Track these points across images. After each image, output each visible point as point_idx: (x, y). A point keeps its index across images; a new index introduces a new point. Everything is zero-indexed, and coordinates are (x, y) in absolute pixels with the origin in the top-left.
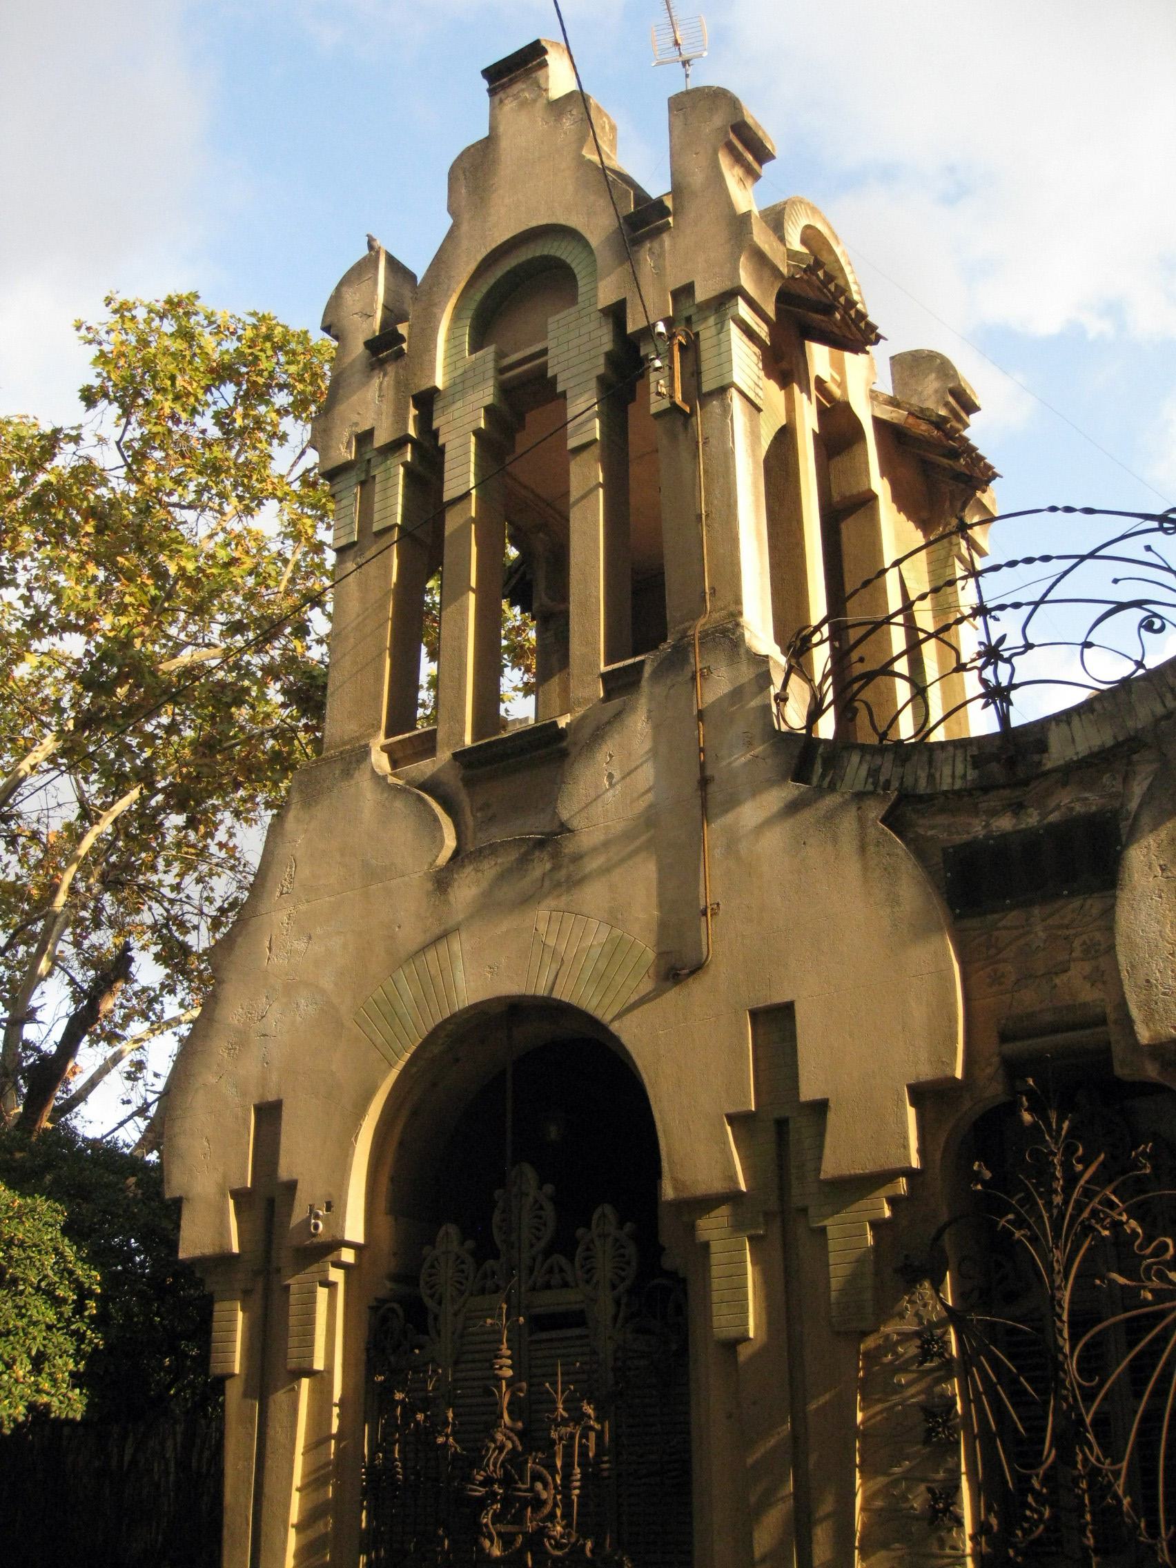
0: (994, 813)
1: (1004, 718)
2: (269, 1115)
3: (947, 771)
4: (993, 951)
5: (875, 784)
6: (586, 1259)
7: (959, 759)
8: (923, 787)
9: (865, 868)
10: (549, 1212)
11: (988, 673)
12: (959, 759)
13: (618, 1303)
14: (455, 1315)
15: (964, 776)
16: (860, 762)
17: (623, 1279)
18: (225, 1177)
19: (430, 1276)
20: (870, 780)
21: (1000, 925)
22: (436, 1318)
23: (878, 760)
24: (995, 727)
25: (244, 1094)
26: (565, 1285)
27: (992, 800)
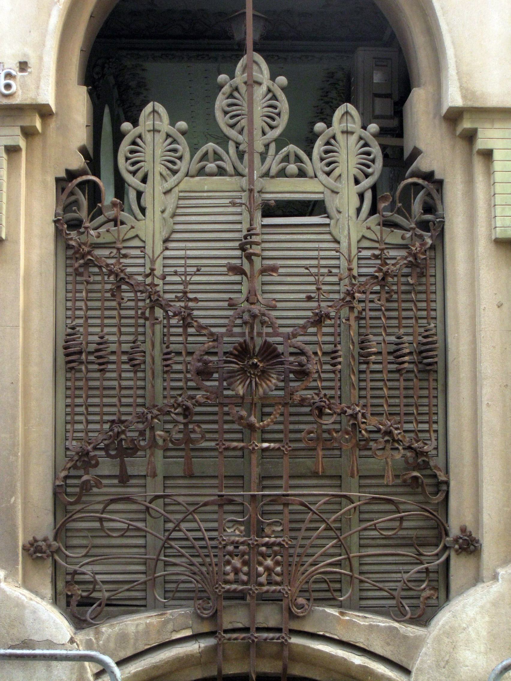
6: (326, 152)
10: (284, 105)
13: (361, 196)
17: (367, 176)
19: (132, 152)
22: (139, 194)
26: (302, 174)
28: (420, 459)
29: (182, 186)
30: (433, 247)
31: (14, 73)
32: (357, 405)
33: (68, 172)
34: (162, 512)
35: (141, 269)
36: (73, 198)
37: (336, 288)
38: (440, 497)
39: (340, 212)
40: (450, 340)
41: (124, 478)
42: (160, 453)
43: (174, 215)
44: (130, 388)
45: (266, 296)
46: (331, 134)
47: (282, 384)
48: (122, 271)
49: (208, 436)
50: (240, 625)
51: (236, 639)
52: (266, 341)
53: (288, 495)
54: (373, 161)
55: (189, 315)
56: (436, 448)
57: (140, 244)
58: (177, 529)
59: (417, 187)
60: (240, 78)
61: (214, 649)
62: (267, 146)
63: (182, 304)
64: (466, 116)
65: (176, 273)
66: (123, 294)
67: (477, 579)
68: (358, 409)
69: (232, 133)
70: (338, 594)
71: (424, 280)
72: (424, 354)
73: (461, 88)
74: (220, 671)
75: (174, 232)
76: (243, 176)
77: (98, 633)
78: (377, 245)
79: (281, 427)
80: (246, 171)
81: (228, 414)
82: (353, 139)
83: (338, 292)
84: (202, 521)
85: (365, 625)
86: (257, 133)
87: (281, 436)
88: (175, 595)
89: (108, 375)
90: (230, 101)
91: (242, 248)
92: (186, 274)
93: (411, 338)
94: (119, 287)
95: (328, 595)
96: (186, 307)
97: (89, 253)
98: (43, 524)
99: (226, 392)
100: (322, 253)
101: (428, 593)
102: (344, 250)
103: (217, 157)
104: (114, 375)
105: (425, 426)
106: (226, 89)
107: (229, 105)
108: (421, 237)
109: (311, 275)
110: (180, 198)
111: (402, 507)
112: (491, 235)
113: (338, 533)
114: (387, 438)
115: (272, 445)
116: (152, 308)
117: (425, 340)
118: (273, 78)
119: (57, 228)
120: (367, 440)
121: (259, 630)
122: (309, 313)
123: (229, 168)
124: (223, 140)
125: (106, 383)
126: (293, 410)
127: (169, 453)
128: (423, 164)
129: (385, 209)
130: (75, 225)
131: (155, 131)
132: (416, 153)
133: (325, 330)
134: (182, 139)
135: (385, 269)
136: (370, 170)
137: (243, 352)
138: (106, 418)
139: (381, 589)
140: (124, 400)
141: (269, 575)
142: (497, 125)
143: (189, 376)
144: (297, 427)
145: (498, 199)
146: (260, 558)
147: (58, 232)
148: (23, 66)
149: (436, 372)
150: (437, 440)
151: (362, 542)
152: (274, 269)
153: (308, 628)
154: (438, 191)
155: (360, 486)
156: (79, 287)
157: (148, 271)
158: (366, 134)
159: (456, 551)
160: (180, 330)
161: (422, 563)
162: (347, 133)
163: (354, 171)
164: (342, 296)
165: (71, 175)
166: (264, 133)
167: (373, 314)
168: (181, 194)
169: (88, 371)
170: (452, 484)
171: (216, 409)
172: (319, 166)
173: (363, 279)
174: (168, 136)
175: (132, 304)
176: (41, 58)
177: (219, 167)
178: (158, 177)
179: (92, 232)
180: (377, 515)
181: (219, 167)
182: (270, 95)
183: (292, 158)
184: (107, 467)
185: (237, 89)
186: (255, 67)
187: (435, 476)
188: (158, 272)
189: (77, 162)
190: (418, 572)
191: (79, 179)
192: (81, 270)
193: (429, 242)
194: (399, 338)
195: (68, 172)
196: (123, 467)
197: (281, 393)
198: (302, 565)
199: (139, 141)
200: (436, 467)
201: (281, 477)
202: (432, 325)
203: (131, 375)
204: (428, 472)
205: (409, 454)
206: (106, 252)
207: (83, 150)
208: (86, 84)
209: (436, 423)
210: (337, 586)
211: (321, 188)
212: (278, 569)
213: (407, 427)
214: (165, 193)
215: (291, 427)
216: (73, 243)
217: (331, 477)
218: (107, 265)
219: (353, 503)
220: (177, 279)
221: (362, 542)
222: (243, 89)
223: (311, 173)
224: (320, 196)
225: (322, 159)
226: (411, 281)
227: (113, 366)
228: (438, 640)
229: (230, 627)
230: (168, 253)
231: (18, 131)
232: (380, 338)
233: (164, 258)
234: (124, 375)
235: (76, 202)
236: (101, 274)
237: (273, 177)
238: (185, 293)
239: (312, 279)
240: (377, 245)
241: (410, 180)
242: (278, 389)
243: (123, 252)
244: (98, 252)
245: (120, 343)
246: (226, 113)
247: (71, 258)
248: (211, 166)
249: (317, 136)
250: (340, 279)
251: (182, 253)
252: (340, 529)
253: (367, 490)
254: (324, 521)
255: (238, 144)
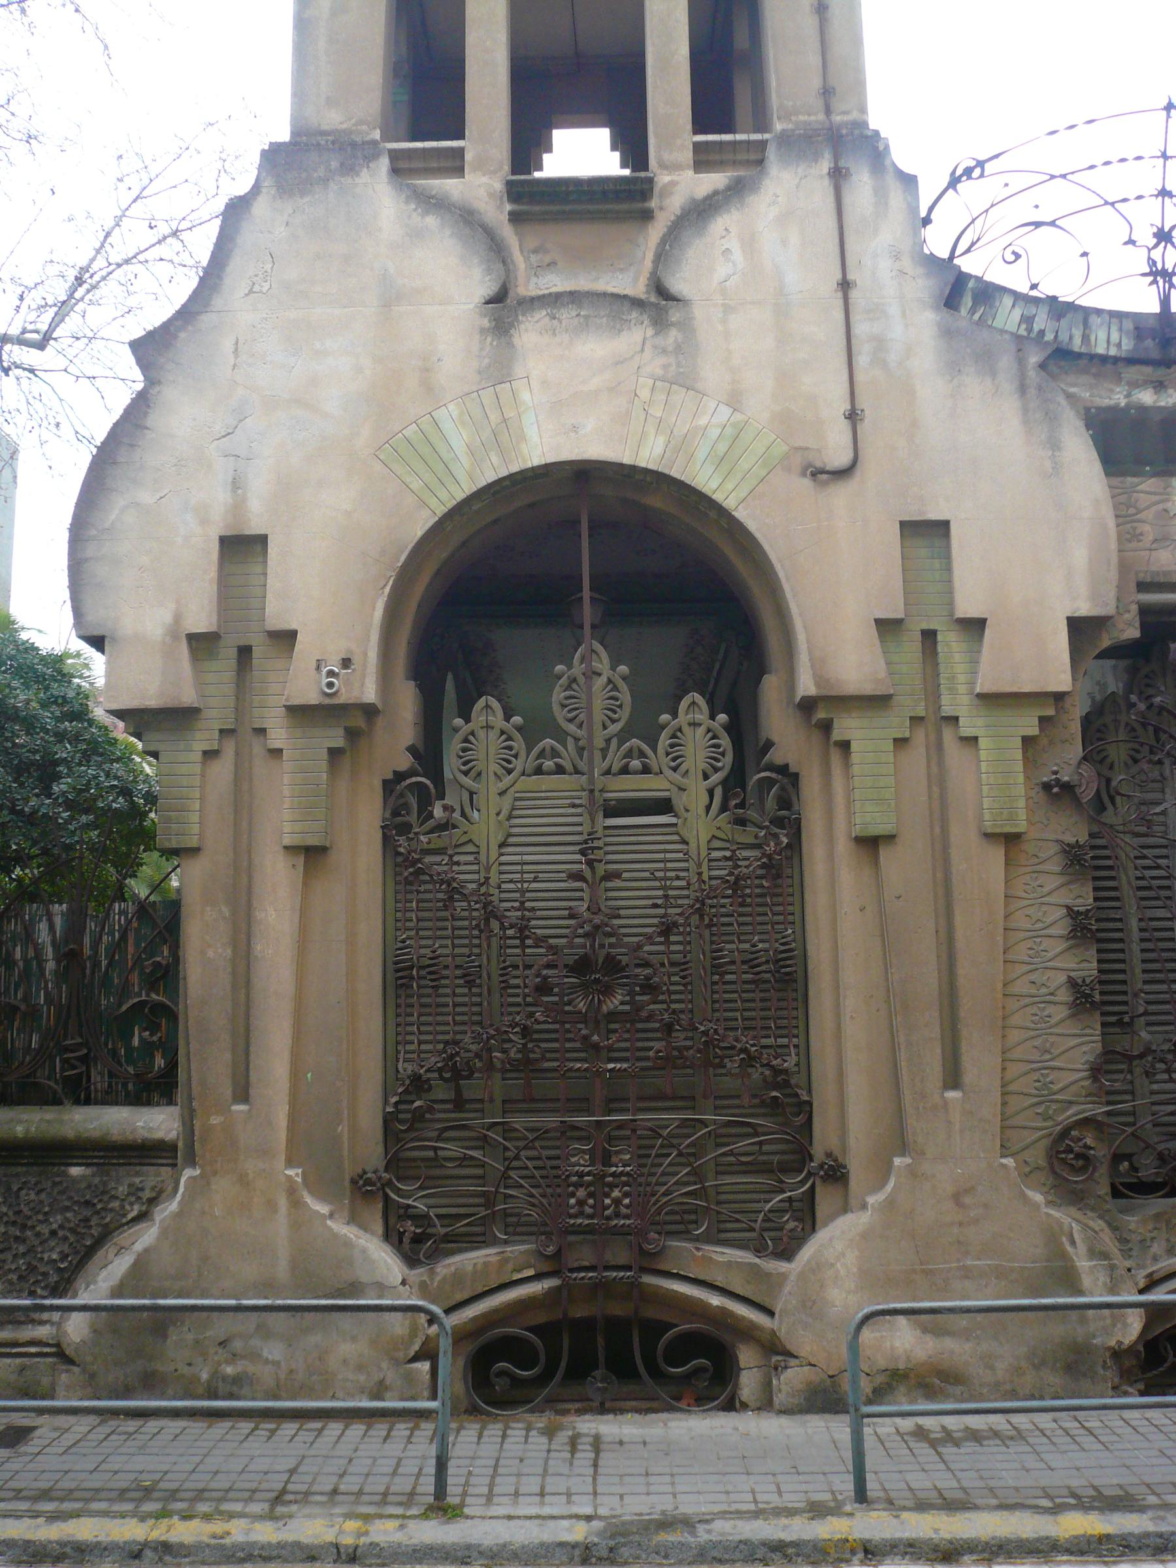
0: (1134, 385)
1: (1165, 302)
2: (241, 549)
3: (1102, 335)
4: (1132, 511)
5: (1030, 330)
6: (672, 746)
7: (1114, 328)
8: (1077, 345)
9: (1025, 410)
10: (626, 697)
11: (1156, 255)
12: (1114, 328)
13: (711, 793)
14: (502, 793)
15: (1119, 345)
16: (1013, 306)
17: (716, 770)
18: (178, 618)
19: (464, 750)
20: (1024, 326)
21: (1139, 488)
23: (1033, 310)
24: (1155, 308)
25: (204, 522)
26: (646, 770)
27: (1132, 372)
28: (780, 1079)
29: (518, 786)
30: (789, 846)
31: (336, 670)
32: (710, 1021)
33: (395, 772)
34: (501, 1140)
35: (476, 877)
36: (402, 801)
37: (685, 892)
38: (799, 1120)
39: (687, 811)
40: (809, 947)
41: (459, 1103)
42: (498, 1076)
43: (510, 817)
44: (465, 1005)
45: (610, 903)
46: (677, 726)
47: (628, 998)
48: (454, 879)
49: (548, 1055)
50: (586, 1263)
51: (583, 1278)
52: (609, 953)
53: (635, 1120)
54: (723, 754)
55: (526, 926)
56: (797, 1065)
57: (474, 849)
58: (517, 1157)
59: (771, 782)
60: (578, 669)
61: (558, 1289)
62: (608, 741)
63: (519, 913)
64: (821, 705)
65: (511, 881)
66: (456, 904)
67: (845, 1209)
68: (711, 1025)
69: (571, 728)
70: (694, 1226)
71: (779, 881)
72: (782, 963)
73: (815, 675)
74: (565, 1315)
75: (510, 835)
76: (583, 774)
77: (432, 1272)
78: (728, 845)
79: (628, 1044)
80: (585, 769)
81: (568, 1031)
82: (701, 731)
83: (688, 897)
84: (542, 1148)
85: (727, 1259)
86: (598, 727)
87: (628, 1054)
88: (516, 1228)
89: (441, 991)
90: (568, 693)
91: (583, 852)
92: (522, 881)
93: (767, 945)
94: (451, 898)
95: (681, 1227)
96: (523, 918)
97: (419, 861)
98: (371, 1153)
99: (567, 1008)
100: (668, 856)
101: (792, 1225)
102: (693, 853)
103: (555, 754)
104: (448, 991)
105: (785, 1041)
106: (563, 681)
107: (567, 698)
108: (776, 836)
109: (656, 879)
110: (516, 799)
111: (760, 1130)
112: (851, 832)
113: (692, 1159)
114: (742, 1056)
115: (619, 1066)
116: (487, 920)
117: (783, 948)
118: (613, 668)
119: (384, 834)
120: (722, 1058)
121: (607, 1268)
122: (655, 921)
123: (568, 766)
124: (561, 735)
125: (439, 1000)
126: (640, 1026)
127: (508, 1076)
128: (776, 756)
129: (736, 806)
130: (404, 829)
131: (488, 727)
132: (769, 745)
133: (673, 938)
134: (517, 735)
135: (736, 872)
136: (720, 764)
137: (582, 966)
138: (440, 1037)
139: (738, 1221)
140: (458, 1018)
141: (617, 1206)
142: (854, 715)
143: (527, 990)
144: (647, 1044)
145: (857, 794)
146: (606, 1189)
147: (386, 839)
148: (346, 663)
149: (796, 981)
150: (798, 1055)
151: (719, 1168)
152: (617, 875)
153: (659, 1267)
154: (793, 785)
155: (716, 1108)
156: (409, 896)
157: (482, 880)
158: (715, 725)
159: (822, 1177)
160: (517, 942)
161: (783, 1191)
162: (694, 725)
163: (702, 765)
164: (691, 902)
165: (399, 776)
166: (605, 727)
167: (723, 920)
168: (517, 795)
169: (419, 987)
170: (815, 1105)
171: (557, 1026)
172: (665, 761)
173: (714, 882)
174: (502, 733)
175: (466, 914)
176: (365, 654)
177: (556, 764)
178: (492, 778)
179: (422, 838)
180: (734, 1139)
181: (556, 764)
182: (610, 686)
183: (636, 753)
184: (441, 1092)
185: (575, 680)
186: (594, 656)
187: (797, 1095)
188: (494, 879)
189: (405, 762)
190: (781, 1201)
191: (408, 781)
192: (411, 878)
193: (785, 840)
194: (754, 946)
195: (395, 772)
196: (458, 1091)
197: (627, 1008)
198: (654, 1195)
199: (471, 738)
200: (797, 1086)
201: (627, 1100)
202: (790, 931)
203: (466, 990)
204: (789, 1091)
205: (767, 1073)
206: (438, 859)
207: (412, 750)
208: (415, 680)
209: (797, 1037)
210: (693, 1217)
211: (667, 785)
212: (627, 1201)
213: (764, 1041)
214: (500, 794)
215: (640, 1044)
216: (402, 850)
217: (682, 1098)
218: (439, 874)
219: (707, 1127)
220: (512, 886)
221: (719, 1168)
222: (581, 680)
223: (656, 769)
224: (667, 793)
225: (668, 754)
226: (765, 884)
227: (446, 982)
228: (802, 1276)
229: (576, 1265)
230: (503, 858)
231: (341, 732)
232: (733, 946)
233: (500, 864)
234: (458, 991)
235: (406, 806)
236: (432, 881)
237: (614, 775)
238: (522, 903)
239: (657, 884)
240: (728, 845)
241: (763, 774)
242: (622, 1003)
243: (455, 859)
244: (428, 859)
245: (454, 956)
246: (564, 706)
247: (400, 866)
248: (549, 764)
249: (663, 727)
250: (689, 884)
251: (518, 858)
252: (693, 1154)
253: (724, 1111)
254: (673, 1146)
255: (577, 740)
